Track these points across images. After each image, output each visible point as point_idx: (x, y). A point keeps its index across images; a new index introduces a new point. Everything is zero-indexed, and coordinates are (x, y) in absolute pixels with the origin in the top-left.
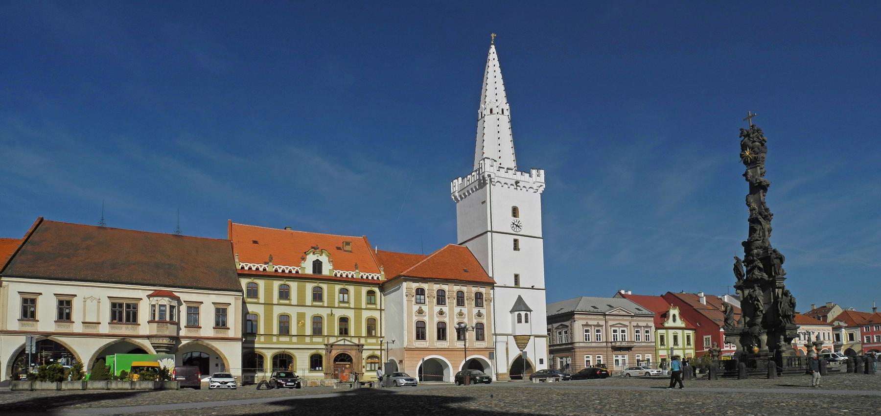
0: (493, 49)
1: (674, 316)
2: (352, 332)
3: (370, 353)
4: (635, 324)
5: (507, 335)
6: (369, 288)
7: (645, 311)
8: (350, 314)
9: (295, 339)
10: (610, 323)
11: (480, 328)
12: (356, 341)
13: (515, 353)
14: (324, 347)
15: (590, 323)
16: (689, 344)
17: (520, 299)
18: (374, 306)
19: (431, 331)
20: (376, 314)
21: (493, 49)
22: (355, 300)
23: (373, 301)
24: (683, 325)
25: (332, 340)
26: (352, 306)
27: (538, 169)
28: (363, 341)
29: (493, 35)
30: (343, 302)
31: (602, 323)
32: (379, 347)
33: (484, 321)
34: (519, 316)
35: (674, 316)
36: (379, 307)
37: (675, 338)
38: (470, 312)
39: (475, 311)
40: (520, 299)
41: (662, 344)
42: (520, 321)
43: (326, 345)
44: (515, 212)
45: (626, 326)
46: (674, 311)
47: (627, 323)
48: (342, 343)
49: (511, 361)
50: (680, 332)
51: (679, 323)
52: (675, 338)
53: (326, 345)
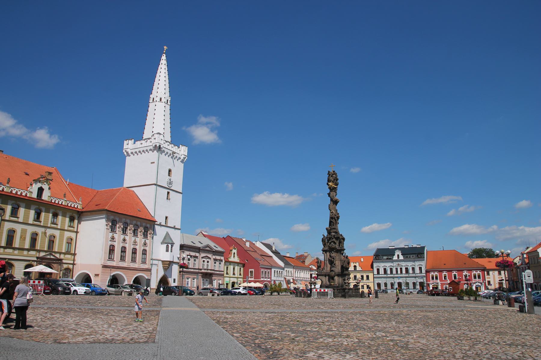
0: (164, 57)
1: (234, 253)
2: (56, 249)
7: (220, 249)
8: (57, 233)
12: (57, 255)
14: (35, 259)
16: (240, 274)
17: (167, 234)
18: (72, 229)
21: (164, 57)
22: (62, 222)
23: (72, 225)
24: (238, 261)
25: (42, 254)
28: (62, 256)
29: (165, 47)
32: (72, 262)
33: (147, 249)
34: (167, 246)
35: (234, 253)
38: (140, 241)
39: (122, 237)
40: (167, 234)
42: (167, 251)
45: (210, 258)
46: (235, 251)
48: (49, 257)
51: (236, 259)
53: (38, 258)
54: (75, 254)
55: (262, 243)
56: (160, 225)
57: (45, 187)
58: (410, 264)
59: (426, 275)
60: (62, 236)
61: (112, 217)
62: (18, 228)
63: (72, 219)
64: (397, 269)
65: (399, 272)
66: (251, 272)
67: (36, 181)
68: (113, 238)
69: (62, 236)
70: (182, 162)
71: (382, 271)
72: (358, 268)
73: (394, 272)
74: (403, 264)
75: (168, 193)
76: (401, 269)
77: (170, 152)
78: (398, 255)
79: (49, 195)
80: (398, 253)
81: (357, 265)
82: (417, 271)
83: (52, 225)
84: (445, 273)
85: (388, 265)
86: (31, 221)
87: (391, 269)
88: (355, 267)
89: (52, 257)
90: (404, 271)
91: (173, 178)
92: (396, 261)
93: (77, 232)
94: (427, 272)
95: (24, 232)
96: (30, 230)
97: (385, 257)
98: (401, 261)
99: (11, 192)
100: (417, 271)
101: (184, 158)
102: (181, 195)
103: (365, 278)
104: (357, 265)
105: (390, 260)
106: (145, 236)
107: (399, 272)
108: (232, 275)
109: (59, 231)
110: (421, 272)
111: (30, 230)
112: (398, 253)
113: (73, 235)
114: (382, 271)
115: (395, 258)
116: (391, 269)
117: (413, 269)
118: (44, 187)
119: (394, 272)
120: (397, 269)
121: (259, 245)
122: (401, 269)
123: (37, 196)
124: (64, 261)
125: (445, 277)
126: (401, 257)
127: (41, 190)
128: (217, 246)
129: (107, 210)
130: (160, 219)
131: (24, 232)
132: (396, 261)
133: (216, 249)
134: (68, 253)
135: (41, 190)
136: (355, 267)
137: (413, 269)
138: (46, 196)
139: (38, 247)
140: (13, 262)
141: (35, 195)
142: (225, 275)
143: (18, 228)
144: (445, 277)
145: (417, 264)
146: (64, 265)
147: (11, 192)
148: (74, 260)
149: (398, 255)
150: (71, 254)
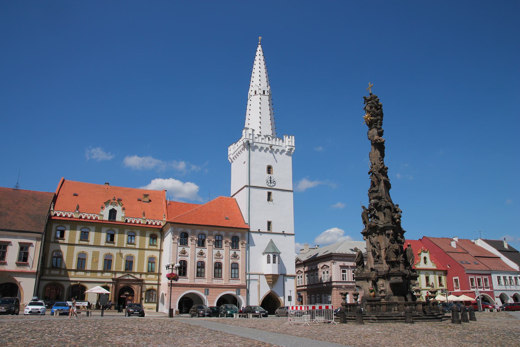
1: (425, 258)
2: (135, 269)
5: (260, 274)
6: (152, 232)
9: (89, 274)
11: (235, 267)
12: (138, 276)
13: (266, 290)
14: (111, 281)
18: (154, 247)
19: (209, 270)
20: (156, 254)
23: (155, 243)
24: (435, 267)
25: (118, 275)
27: (292, 136)
28: (144, 277)
30: (131, 244)
32: (157, 282)
35: (425, 258)
36: (159, 248)
43: (113, 279)
44: (269, 169)
48: (127, 278)
49: (262, 297)
53: (113, 279)
55: (483, 240)
56: (259, 232)
57: (118, 208)
60: (141, 257)
61: (181, 230)
62: (89, 251)
63: (153, 237)
67: (107, 203)
68: (184, 253)
69: (141, 257)
70: (288, 154)
75: (269, 194)
77: (265, 146)
79: (123, 215)
83: (128, 245)
86: (103, 243)
89: (131, 278)
91: (275, 175)
93: (161, 251)
95: (96, 255)
99: (81, 217)
101: (291, 149)
102: (292, 194)
106: (235, 245)
109: (137, 251)
111: (102, 252)
113: (156, 254)
118: (116, 208)
121: (480, 243)
123: (110, 218)
124: (146, 282)
127: (113, 213)
130: (257, 224)
131: (96, 255)
134: (151, 271)
135: (113, 213)
138: (120, 217)
139: (114, 269)
140: (85, 284)
141: (106, 217)
143: (89, 251)
146: (146, 286)
147: (81, 217)
148: (159, 280)
150: (155, 274)
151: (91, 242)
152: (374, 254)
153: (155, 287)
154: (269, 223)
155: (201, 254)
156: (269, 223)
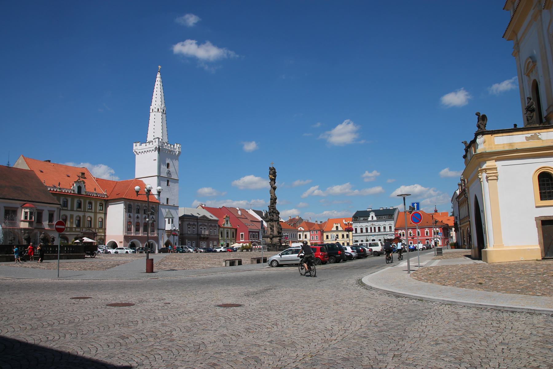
0: (159, 75)
3: (100, 237)
4: (209, 224)
10: (199, 224)
12: (94, 230)
15: (191, 223)
21: (159, 75)
25: (84, 230)
26: (93, 211)
29: (160, 67)
31: (196, 223)
37: (227, 233)
41: (222, 236)
45: (206, 226)
47: (206, 224)
48: (88, 231)
50: (229, 230)
52: (227, 233)
54: (105, 229)
55: (254, 210)
58: (381, 224)
59: (395, 232)
61: (128, 203)
63: (101, 205)
64: (371, 228)
65: (373, 231)
66: (242, 235)
71: (359, 231)
72: (340, 228)
73: (369, 231)
74: (375, 223)
76: (375, 228)
78: (372, 217)
80: (372, 214)
81: (339, 225)
82: (388, 229)
84: (427, 230)
85: (364, 225)
86: (75, 209)
87: (367, 229)
88: (337, 227)
90: (377, 230)
92: (370, 221)
94: (396, 230)
96: (75, 214)
97: (362, 219)
98: (375, 221)
100: (388, 229)
103: (345, 236)
104: (339, 225)
105: (366, 220)
107: (373, 231)
108: (225, 237)
110: (391, 231)
112: (372, 214)
114: (359, 231)
115: (370, 219)
116: (367, 229)
117: (385, 228)
119: (369, 231)
120: (371, 228)
122: (375, 228)
125: (427, 233)
126: (375, 218)
128: (212, 216)
129: (124, 198)
131: (72, 216)
132: (370, 221)
133: (211, 218)
136: (337, 227)
137: (385, 228)
142: (220, 238)
144: (427, 233)
145: (387, 224)
149: (372, 217)
151: (69, 208)
152: (271, 229)
153: (103, 237)
154: (167, 199)
155: (138, 217)
156: (167, 199)
